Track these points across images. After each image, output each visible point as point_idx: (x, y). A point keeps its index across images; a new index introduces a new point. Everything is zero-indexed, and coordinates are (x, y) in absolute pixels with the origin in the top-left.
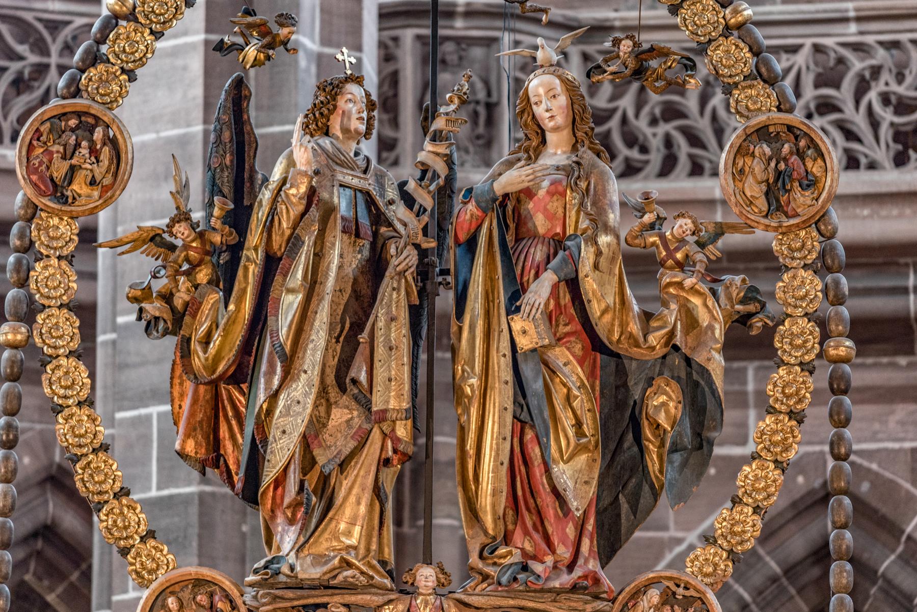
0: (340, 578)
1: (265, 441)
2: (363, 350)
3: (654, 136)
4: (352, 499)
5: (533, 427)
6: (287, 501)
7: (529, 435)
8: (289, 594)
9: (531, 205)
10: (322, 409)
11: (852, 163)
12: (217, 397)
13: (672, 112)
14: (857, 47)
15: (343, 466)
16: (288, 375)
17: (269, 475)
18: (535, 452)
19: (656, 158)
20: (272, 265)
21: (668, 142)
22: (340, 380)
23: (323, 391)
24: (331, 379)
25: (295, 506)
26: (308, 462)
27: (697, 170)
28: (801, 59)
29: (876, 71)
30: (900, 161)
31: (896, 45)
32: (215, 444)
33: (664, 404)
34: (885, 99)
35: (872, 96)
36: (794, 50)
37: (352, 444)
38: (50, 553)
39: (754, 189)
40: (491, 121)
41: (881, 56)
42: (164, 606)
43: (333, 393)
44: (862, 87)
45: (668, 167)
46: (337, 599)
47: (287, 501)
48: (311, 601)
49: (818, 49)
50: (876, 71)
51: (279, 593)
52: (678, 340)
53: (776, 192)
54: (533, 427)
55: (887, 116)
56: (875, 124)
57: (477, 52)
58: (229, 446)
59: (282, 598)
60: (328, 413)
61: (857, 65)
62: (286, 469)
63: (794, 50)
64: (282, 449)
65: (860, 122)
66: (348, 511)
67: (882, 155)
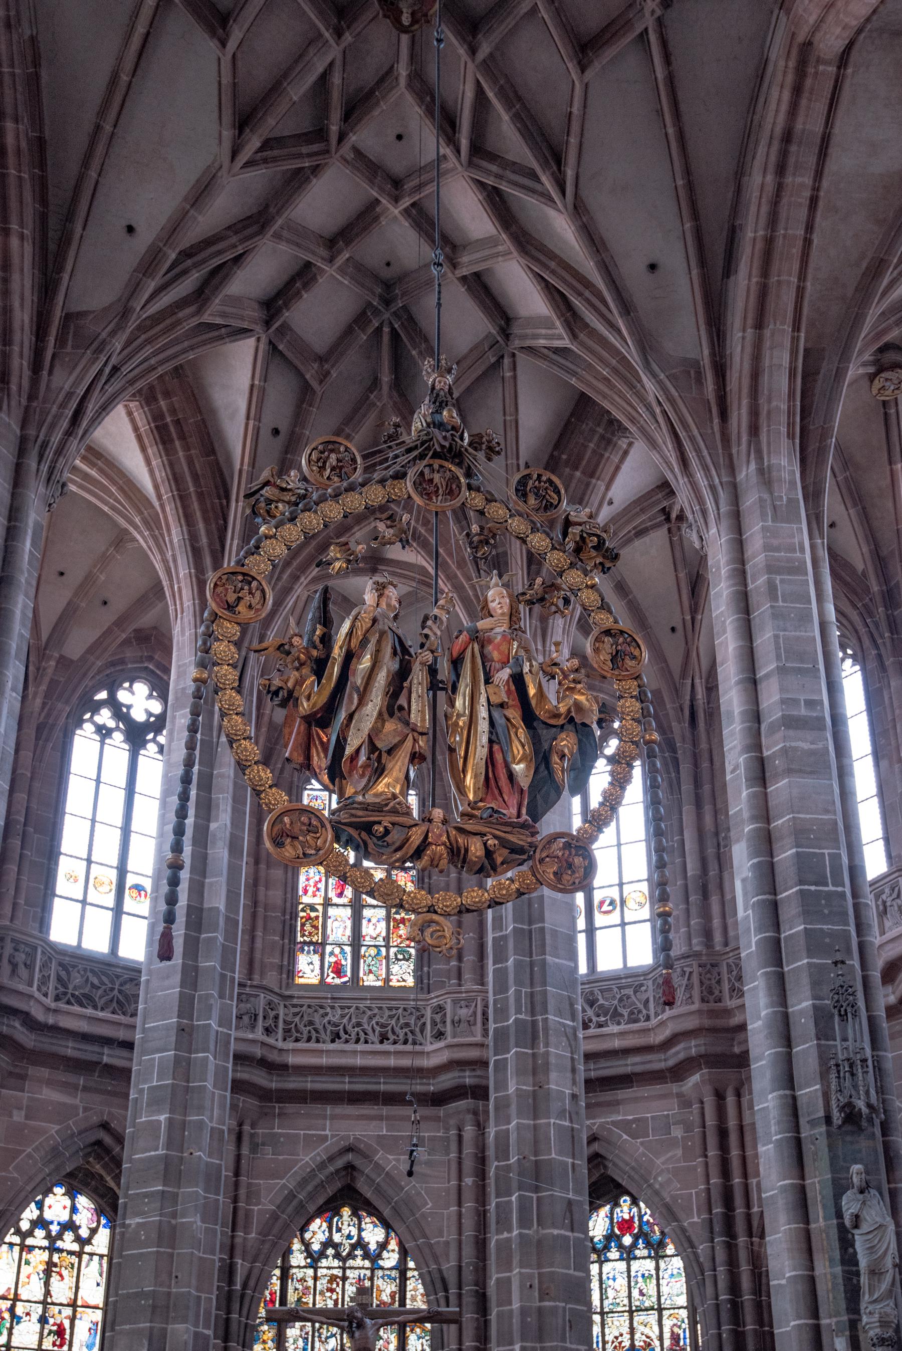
0: (391, 804)
1: (345, 740)
2: (405, 691)
3: (305, 1030)
4: (397, 767)
5: (499, 743)
6: (360, 763)
7: (496, 747)
8: (360, 813)
9: (490, 648)
10: (379, 725)
11: (366, 1042)
12: (309, 737)
13: (311, 1023)
14: (370, 1009)
15: (390, 752)
16: (361, 703)
17: (349, 751)
18: (499, 757)
19: (305, 1036)
20: (349, 657)
21: (309, 1032)
22: (394, 707)
23: (380, 714)
24: (384, 709)
25: (365, 767)
26: (373, 748)
27: (318, 1041)
28: (352, 1010)
29: (375, 1015)
30: (381, 1042)
31: (380, 1008)
32: (308, 757)
33: (566, 742)
34: (377, 1023)
35: (374, 1022)
36: (349, 1008)
37: (398, 739)
38: (99, 1151)
39: (605, 656)
40: (255, 1020)
41: (376, 1011)
42: (282, 822)
43: (386, 716)
44: (370, 1018)
45: (309, 1040)
46: (388, 818)
47: (360, 763)
48: (372, 819)
49: (357, 1008)
50: (375, 1015)
51: (353, 812)
52: (573, 714)
53: (616, 658)
54: (499, 743)
55: (378, 1029)
56: (374, 1031)
57: (252, 999)
58: (316, 758)
59: (356, 816)
60: (383, 727)
61: (369, 1013)
62: (358, 751)
63: (349, 1008)
64: (353, 742)
65: (370, 1031)
66: (395, 774)
67: (376, 1040)
